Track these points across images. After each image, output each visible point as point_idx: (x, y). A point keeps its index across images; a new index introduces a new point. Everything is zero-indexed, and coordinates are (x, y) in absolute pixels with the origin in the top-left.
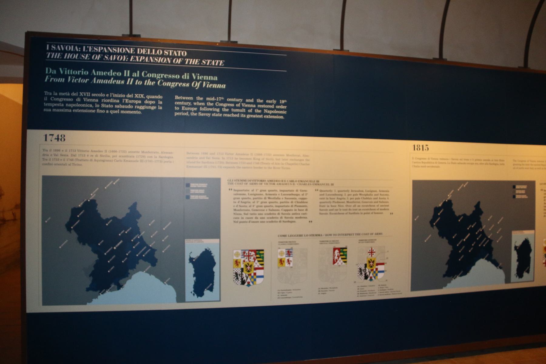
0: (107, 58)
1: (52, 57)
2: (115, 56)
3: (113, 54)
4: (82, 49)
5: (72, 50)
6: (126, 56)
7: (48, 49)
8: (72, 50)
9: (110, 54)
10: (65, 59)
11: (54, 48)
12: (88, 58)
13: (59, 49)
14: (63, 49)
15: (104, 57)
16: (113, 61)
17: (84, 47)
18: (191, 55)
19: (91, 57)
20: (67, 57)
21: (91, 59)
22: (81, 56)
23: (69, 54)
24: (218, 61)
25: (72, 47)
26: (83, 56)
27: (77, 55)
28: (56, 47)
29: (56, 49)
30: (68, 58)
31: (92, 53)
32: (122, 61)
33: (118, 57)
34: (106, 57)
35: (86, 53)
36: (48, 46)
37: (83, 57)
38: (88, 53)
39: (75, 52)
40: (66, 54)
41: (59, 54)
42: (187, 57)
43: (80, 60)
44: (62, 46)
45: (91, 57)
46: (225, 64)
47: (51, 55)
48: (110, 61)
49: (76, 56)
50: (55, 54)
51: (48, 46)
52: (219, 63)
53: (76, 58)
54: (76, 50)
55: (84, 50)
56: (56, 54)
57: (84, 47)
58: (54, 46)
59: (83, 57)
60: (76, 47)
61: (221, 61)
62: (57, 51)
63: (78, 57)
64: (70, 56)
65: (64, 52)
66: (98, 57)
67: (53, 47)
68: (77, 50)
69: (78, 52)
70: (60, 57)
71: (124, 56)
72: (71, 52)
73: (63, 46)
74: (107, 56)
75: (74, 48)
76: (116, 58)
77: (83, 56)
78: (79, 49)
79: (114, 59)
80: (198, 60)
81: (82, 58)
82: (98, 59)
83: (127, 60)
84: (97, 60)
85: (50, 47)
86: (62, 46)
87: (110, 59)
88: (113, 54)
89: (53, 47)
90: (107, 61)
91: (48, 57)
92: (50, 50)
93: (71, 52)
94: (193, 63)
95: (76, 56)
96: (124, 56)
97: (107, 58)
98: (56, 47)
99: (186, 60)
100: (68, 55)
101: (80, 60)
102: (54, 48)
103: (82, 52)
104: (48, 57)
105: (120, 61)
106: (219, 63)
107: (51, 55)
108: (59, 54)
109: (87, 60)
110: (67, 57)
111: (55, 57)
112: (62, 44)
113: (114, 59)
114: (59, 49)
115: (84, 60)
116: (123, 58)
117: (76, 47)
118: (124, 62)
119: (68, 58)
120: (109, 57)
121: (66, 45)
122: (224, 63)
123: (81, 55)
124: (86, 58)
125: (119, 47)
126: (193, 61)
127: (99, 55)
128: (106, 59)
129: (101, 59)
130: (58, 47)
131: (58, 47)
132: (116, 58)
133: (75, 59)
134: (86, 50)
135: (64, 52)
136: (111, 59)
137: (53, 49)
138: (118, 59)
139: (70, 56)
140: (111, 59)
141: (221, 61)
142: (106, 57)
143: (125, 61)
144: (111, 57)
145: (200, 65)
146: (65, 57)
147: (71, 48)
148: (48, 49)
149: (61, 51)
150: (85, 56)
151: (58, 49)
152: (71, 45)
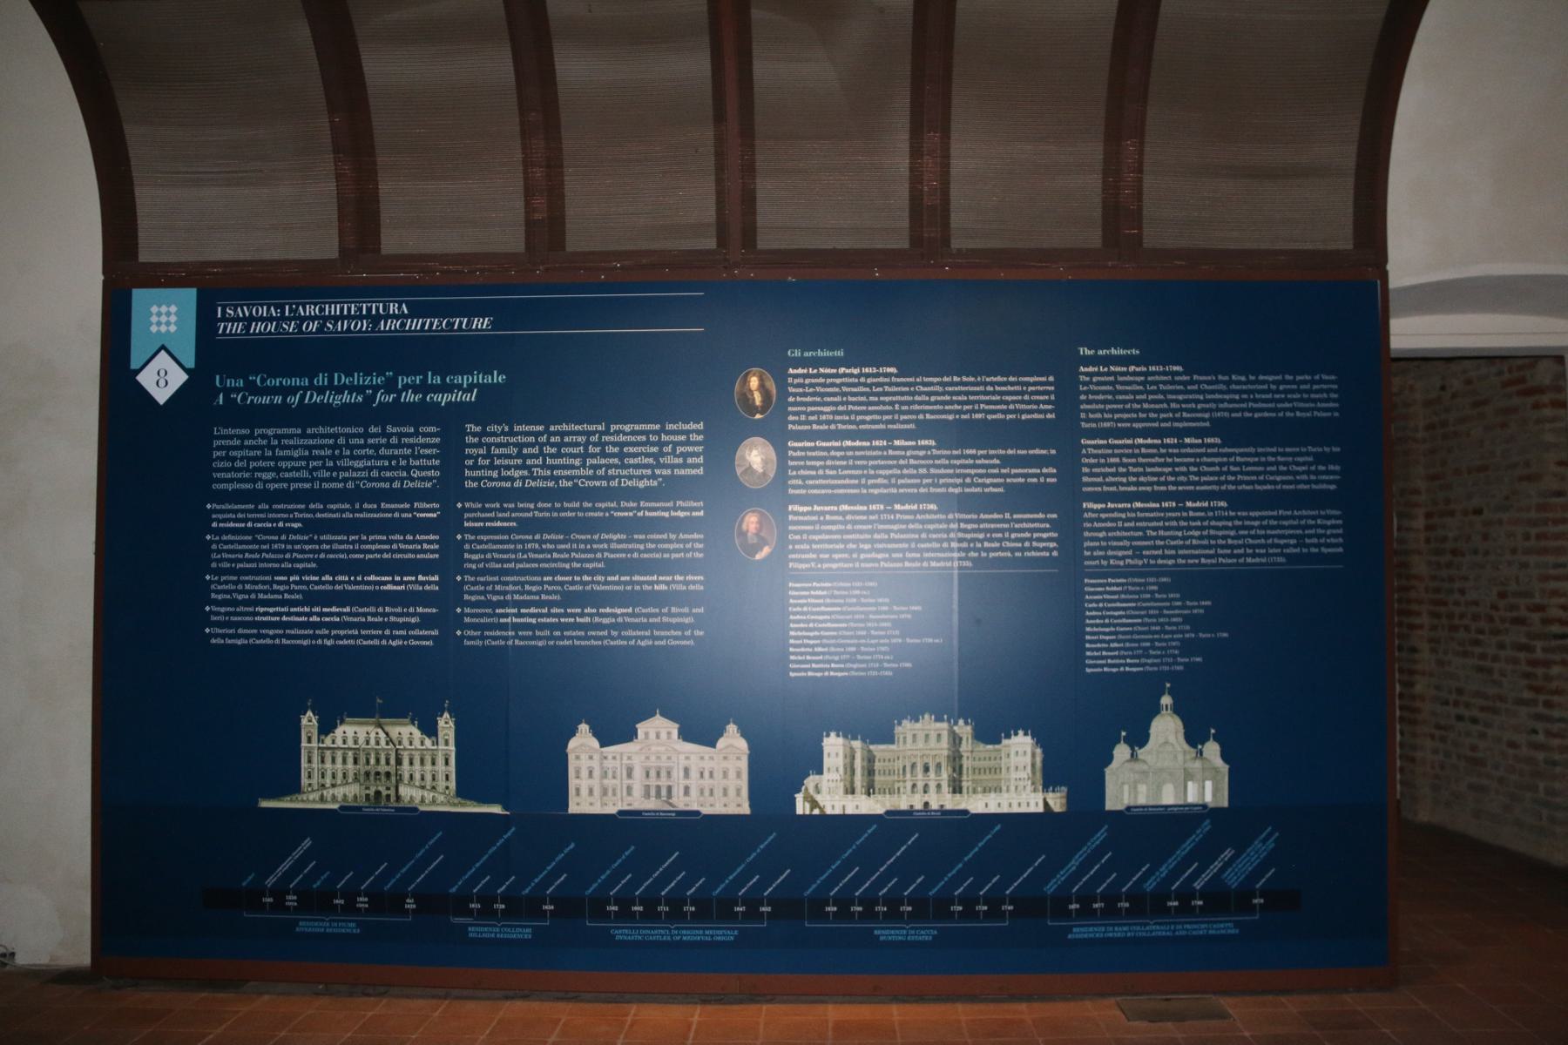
0: (331, 326)
1: (228, 332)
4: (283, 312)
7: (219, 316)
11: (232, 312)
12: (294, 329)
13: (241, 315)
14: (247, 314)
15: (325, 324)
16: (342, 332)
17: (287, 307)
19: (300, 327)
20: (255, 329)
21: (301, 332)
25: (265, 308)
26: (284, 326)
28: (235, 311)
31: (303, 319)
32: (360, 331)
34: (328, 325)
35: (290, 319)
36: (220, 309)
38: (294, 318)
39: (270, 319)
42: (406, 317)
43: (280, 334)
44: (245, 308)
47: (225, 328)
48: (337, 332)
49: (272, 327)
50: (233, 326)
51: (220, 309)
55: (287, 314)
57: (287, 307)
60: (272, 309)
62: (238, 320)
64: (260, 327)
66: (314, 326)
70: (242, 330)
72: (262, 319)
75: (268, 309)
76: (349, 327)
77: (284, 326)
78: (277, 313)
81: (284, 329)
84: (311, 333)
85: (224, 312)
86: (245, 308)
89: (228, 311)
90: (331, 333)
91: (220, 332)
92: (224, 319)
93: (262, 319)
95: (272, 327)
97: (331, 326)
98: (235, 311)
100: (256, 325)
101: (280, 334)
102: (232, 312)
103: (283, 318)
104: (220, 332)
105: (357, 332)
107: (225, 328)
109: (293, 333)
110: (255, 329)
114: (241, 315)
115: (288, 333)
116: (362, 325)
117: (272, 309)
120: (335, 325)
121: (254, 305)
122: (492, 323)
125: (333, 303)
126: (412, 322)
128: (329, 328)
129: (320, 330)
130: (239, 309)
131: (239, 309)
132: (349, 327)
134: (290, 313)
138: (352, 327)
139: (260, 327)
142: (328, 325)
143: (367, 332)
144: (339, 323)
145: (372, 331)
146: (252, 331)
147: (263, 311)
148: (219, 316)
149: (244, 319)
150: (289, 326)
152: (262, 306)
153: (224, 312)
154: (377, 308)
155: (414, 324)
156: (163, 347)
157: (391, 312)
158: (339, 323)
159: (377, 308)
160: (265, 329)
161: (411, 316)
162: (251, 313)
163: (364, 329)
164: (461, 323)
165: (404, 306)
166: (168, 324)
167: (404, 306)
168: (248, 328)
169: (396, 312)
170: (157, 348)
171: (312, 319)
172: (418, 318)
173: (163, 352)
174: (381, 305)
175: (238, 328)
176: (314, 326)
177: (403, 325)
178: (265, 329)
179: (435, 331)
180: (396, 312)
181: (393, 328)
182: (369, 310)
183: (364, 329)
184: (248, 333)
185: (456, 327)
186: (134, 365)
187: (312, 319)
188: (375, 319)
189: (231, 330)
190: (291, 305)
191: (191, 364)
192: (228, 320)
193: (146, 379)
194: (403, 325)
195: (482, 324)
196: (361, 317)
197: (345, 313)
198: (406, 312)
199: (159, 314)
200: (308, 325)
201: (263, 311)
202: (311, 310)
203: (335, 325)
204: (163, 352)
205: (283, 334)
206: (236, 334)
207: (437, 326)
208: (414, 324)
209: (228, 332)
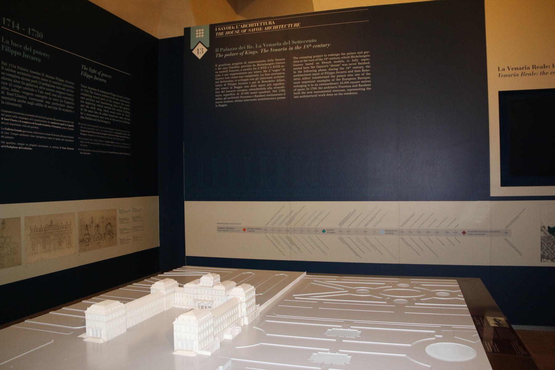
0: (250, 30)
1: (219, 35)
2: (254, 29)
3: (253, 27)
7: (216, 30)
8: (230, 29)
9: (251, 28)
10: (226, 35)
12: (239, 32)
13: (223, 30)
14: (225, 29)
15: (248, 30)
16: (253, 32)
17: (237, 26)
18: (277, 23)
20: (227, 34)
21: (241, 33)
23: (228, 32)
24: (280, 26)
25: (230, 27)
26: (236, 32)
27: (233, 31)
28: (221, 29)
30: (228, 34)
32: (259, 31)
34: (249, 30)
35: (238, 29)
36: (216, 29)
39: (232, 30)
42: (275, 25)
43: (234, 34)
44: (224, 27)
45: (240, 31)
46: (301, 25)
47: (218, 34)
49: (232, 32)
50: (220, 33)
51: (216, 29)
55: (237, 28)
56: (221, 33)
57: (237, 26)
60: (232, 27)
62: (221, 31)
64: (228, 33)
65: (226, 30)
66: (245, 31)
67: (219, 29)
68: (233, 28)
69: (233, 30)
70: (223, 34)
71: (260, 28)
72: (229, 30)
73: (225, 27)
75: (231, 27)
77: (236, 32)
78: (234, 28)
81: (236, 33)
82: (245, 32)
84: (244, 33)
85: (217, 29)
86: (224, 27)
88: (253, 27)
89: (219, 29)
91: (217, 35)
92: (218, 31)
93: (229, 30)
95: (232, 32)
96: (260, 28)
97: (250, 30)
98: (221, 29)
99: (289, 25)
100: (227, 32)
101: (234, 34)
102: (220, 29)
103: (236, 29)
104: (217, 35)
107: (218, 34)
109: (238, 34)
110: (227, 34)
111: (221, 35)
114: (223, 30)
115: (237, 34)
117: (232, 27)
118: (260, 31)
119: (228, 34)
120: (251, 30)
121: (227, 26)
124: (238, 33)
125: (251, 23)
127: (245, 30)
128: (249, 31)
129: (247, 32)
130: (222, 28)
131: (222, 28)
133: (232, 34)
134: (238, 28)
135: (225, 31)
136: (253, 31)
139: (228, 33)
140: (253, 31)
142: (249, 30)
143: (261, 31)
144: (253, 29)
147: (230, 28)
148: (216, 30)
150: (237, 32)
153: (217, 29)
154: (265, 23)
155: (276, 27)
156: (200, 42)
157: (269, 24)
159: (265, 23)
160: (230, 33)
163: (260, 30)
164: (290, 25)
165: (273, 22)
166: (201, 34)
168: (225, 33)
169: (271, 24)
170: (198, 42)
171: (244, 29)
173: (200, 43)
174: (266, 22)
175: (222, 34)
176: (245, 31)
177: (272, 28)
178: (230, 33)
179: (282, 29)
180: (271, 24)
181: (269, 29)
182: (263, 24)
183: (260, 30)
184: (225, 35)
185: (289, 27)
186: (192, 48)
188: (263, 27)
189: (220, 35)
190: (238, 25)
191: (208, 46)
193: (195, 52)
194: (272, 28)
195: (297, 25)
196: (259, 27)
198: (274, 24)
199: (198, 32)
200: (243, 31)
201: (230, 28)
204: (200, 43)
205: (236, 34)
206: (221, 36)
207: (283, 27)
208: (276, 27)
209: (219, 35)
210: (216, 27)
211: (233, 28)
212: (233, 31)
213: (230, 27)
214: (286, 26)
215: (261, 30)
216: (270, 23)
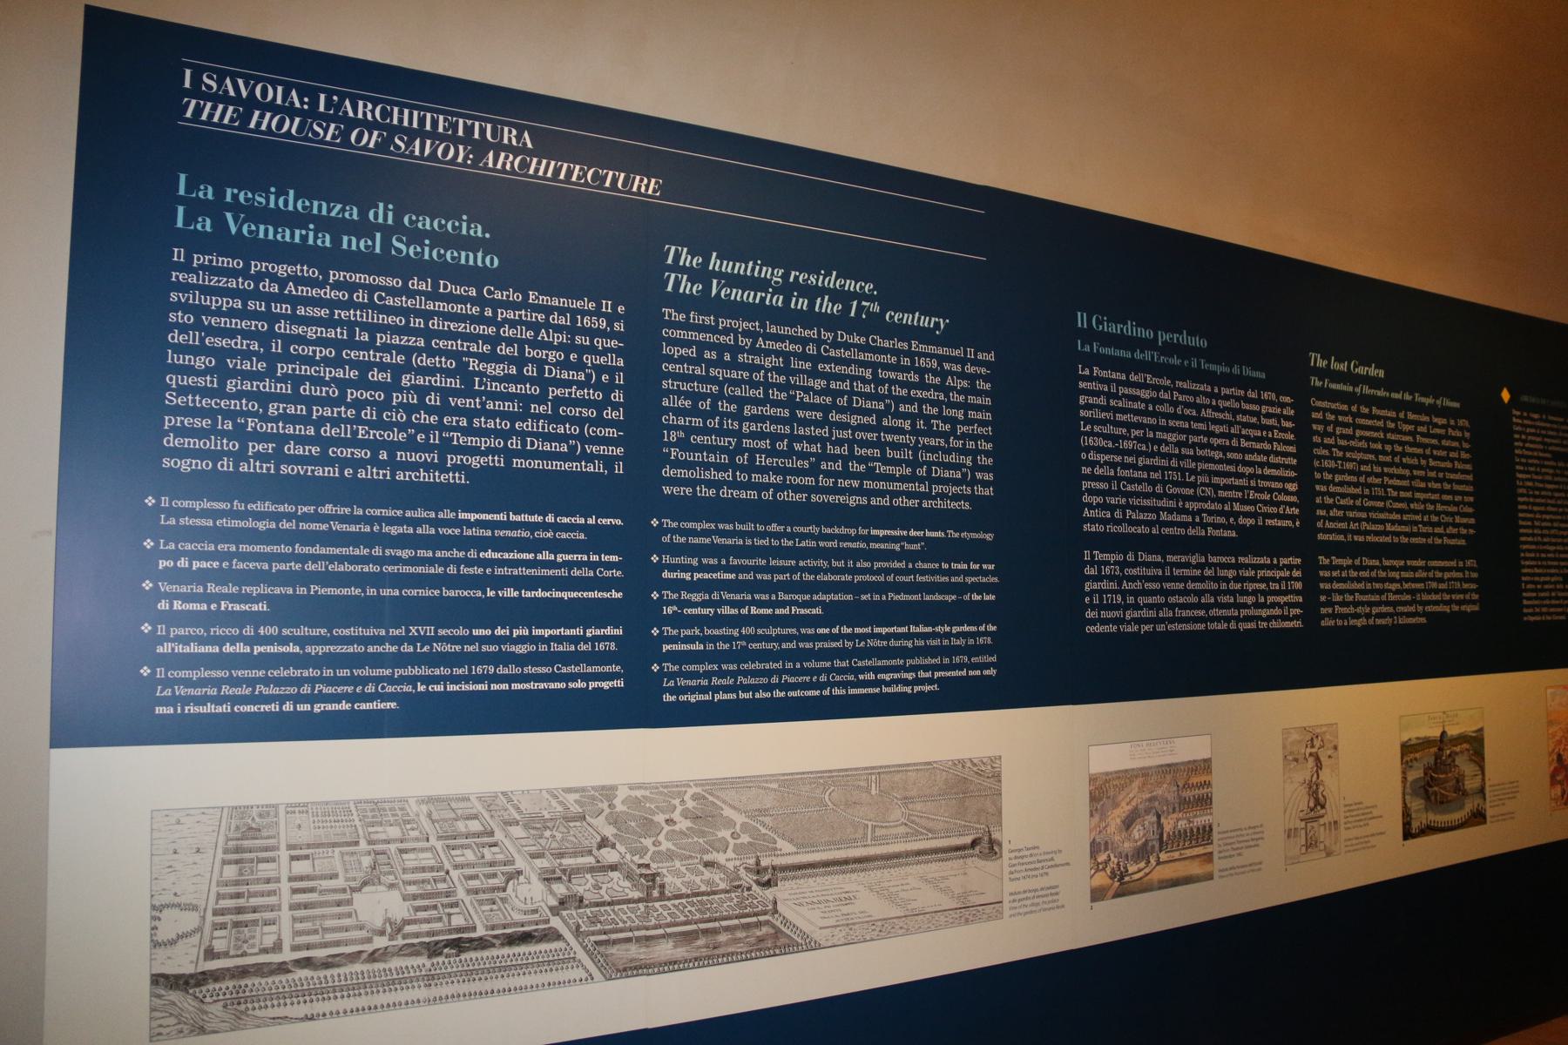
1: (204, 117)
2: (428, 142)
4: (314, 103)
5: (279, 101)
6: (465, 149)
7: (187, 84)
8: (279, 101)
12: (334, 137)
13: (232, 93)
14: (244, 94)
17: (322, 97)
19: (345, 135)
20: (259, 124)
21: (346, 142)
22: (311, 128)
23: (268, 115)
25: (280, 89)
26: (316, 128)
27: (297, 120)
29: (219, 89)
30: (264, 127)
31: (353, 123)
33: (439, 145)
35: (328, 119)
36: (188, 72)
37: (321, 132)
38: (335, 118)
39: (291, 112)
40: (257, 113)
41: (231, 108)
42: (531, 153)
43: (306, 139)
45: (345, 135)
47: (198, 110)
49: (292, 126)
50: (214, 108)
51: (188, 72)
52: (570, 173)
53: (293, 131)
54: (292, 103)
55: (322, 109)
56: (221, 107)
57: (322, 97)
58: (210, 77)
59: (321, 132)
61: (578, 167)
62: (220, 98)
63: (300, 130)
64: (269, 121)
65: (251, 104)
66: (372, 139)
68: (297, 105)
69: (300, 112)
70: (232, 120)
71: (461, 148)
72: (273, 108)
74: (401, 139)
75: (286, 95)
76: (434, 152)
77: (316, 128)
78: (302, 103)
79: (427, 151)
80: (656, 183)
82: (371, 145)
83: (469, 162)
85: (197, 80)
86: (240, 82)
87: (413, 152)
90: (402, 155)
91: (189, 114)
92: (196, 92)
93: (273, 108)
94: (541, 173)
95: (292, 126)
96: (461, 148)
98: (220, 82)
100: (262, 116)
101: (306, 139)
103: (312, 114)
104: (189, 114)
106: (570, 173)
107: (198, 110)
108: (231, 108)
110: (259, 124)
112: (241, 75)
113: (427, 151)
114: (232, 93)
115: (323, 142)
117: (294, 93)
119: (264, 127)
120: (409, 144)
121: (258, 80)
123: (312, 124)
124: (328, 138)
126: (539, 163)
127: (376, 133)
128: (398, 148)
129: (383, 146)
130: (228, 81)
131: (228, 81)
132: (434, 152)
133: (288, 134)
134: (327, 107)
135: (251, 104)
136: (417, 153)
137: (210, 87)
139: (269, 121)
140: (417, 153)
141: (578, 167)
144: (417, 142)
146: (252, 125)
147: (276, 95)
148: (187, 84)
149: (237, 101)
150: (326, 132)
151: (226, 91)
152: (274, 83)
154: (483, 131)
155: (542, 168)
157: (506, 141)
158: (417, 142)
159: (483, 131)
161: (541, 151)
162: (252, 93)
163: (460, 160)
164: (615, 180)
165: (526, 135)
167: (526, 135)
169: (514, 142)
171: (371, 126)
172: (550, 159)
174: (489, 126)
175: (226, 115)
176: (372, 139)
177: (525, 165)
178: (280, 125)
179: (574, 184)
180: (514, 142)
181: (508, 167)
183: (460, 160)
185: (607, 184)
187: (371, 126)
189: (211, 116)
190: (329, 94)
192: (208, 97)
195: (647, 186)
196: (456, 141)
197: (428, 127)
198: (530, 145)
202: (365, 110)
203: (409, 144)
207: (579, 178)
208: (542, 168)
209: (204, 117)
210: (189, 66)
211: (297, 105)
212: (297, 120)
213: (280, 89)
214: (596, 176)
215: (466, 158)
216: (509, 135)
